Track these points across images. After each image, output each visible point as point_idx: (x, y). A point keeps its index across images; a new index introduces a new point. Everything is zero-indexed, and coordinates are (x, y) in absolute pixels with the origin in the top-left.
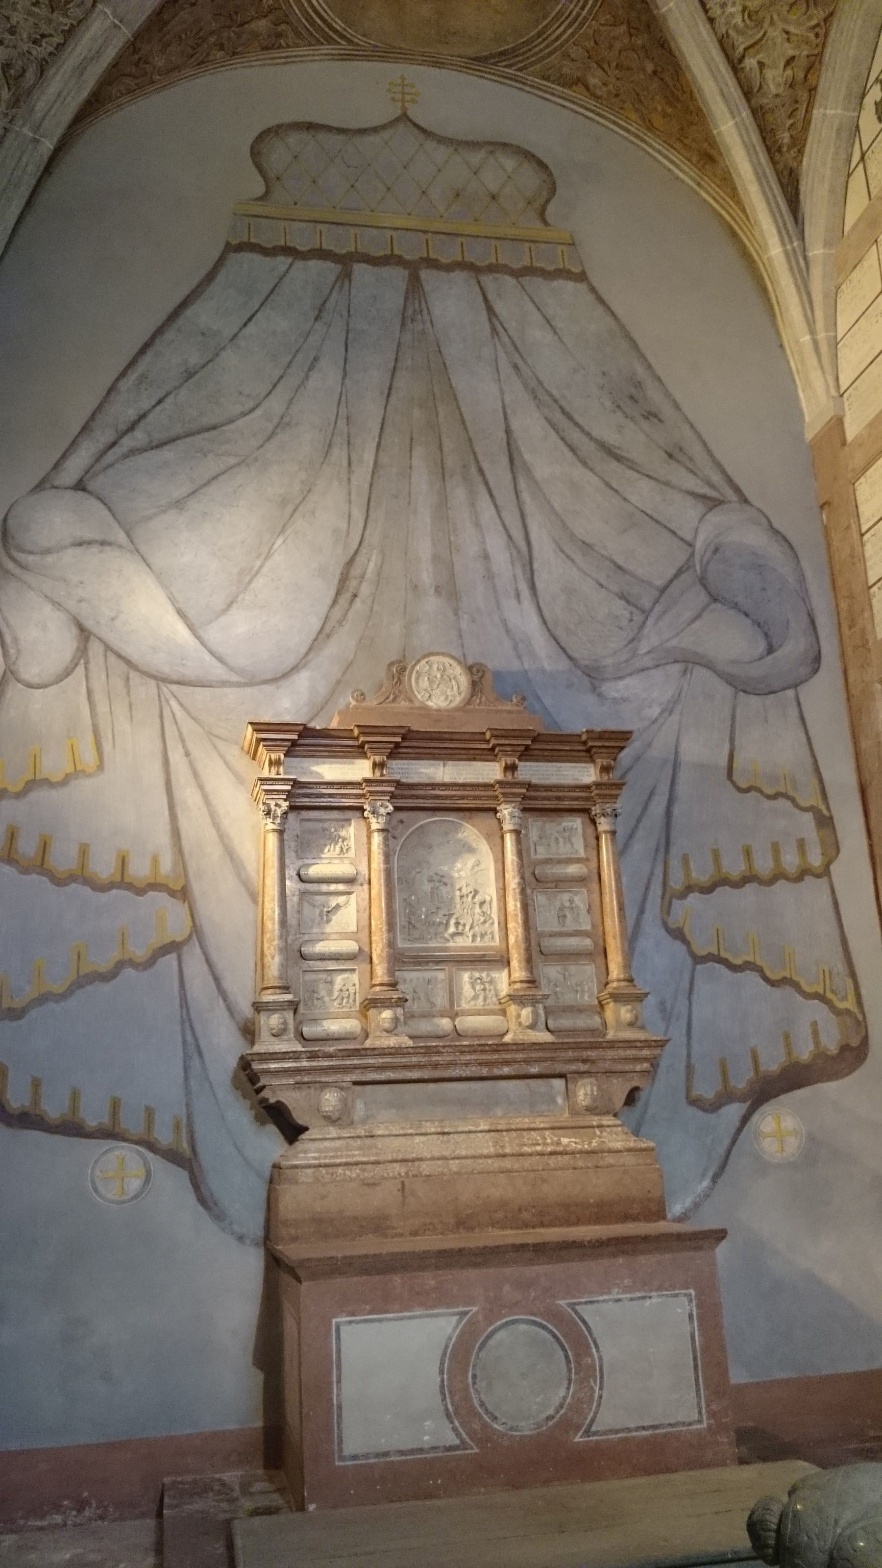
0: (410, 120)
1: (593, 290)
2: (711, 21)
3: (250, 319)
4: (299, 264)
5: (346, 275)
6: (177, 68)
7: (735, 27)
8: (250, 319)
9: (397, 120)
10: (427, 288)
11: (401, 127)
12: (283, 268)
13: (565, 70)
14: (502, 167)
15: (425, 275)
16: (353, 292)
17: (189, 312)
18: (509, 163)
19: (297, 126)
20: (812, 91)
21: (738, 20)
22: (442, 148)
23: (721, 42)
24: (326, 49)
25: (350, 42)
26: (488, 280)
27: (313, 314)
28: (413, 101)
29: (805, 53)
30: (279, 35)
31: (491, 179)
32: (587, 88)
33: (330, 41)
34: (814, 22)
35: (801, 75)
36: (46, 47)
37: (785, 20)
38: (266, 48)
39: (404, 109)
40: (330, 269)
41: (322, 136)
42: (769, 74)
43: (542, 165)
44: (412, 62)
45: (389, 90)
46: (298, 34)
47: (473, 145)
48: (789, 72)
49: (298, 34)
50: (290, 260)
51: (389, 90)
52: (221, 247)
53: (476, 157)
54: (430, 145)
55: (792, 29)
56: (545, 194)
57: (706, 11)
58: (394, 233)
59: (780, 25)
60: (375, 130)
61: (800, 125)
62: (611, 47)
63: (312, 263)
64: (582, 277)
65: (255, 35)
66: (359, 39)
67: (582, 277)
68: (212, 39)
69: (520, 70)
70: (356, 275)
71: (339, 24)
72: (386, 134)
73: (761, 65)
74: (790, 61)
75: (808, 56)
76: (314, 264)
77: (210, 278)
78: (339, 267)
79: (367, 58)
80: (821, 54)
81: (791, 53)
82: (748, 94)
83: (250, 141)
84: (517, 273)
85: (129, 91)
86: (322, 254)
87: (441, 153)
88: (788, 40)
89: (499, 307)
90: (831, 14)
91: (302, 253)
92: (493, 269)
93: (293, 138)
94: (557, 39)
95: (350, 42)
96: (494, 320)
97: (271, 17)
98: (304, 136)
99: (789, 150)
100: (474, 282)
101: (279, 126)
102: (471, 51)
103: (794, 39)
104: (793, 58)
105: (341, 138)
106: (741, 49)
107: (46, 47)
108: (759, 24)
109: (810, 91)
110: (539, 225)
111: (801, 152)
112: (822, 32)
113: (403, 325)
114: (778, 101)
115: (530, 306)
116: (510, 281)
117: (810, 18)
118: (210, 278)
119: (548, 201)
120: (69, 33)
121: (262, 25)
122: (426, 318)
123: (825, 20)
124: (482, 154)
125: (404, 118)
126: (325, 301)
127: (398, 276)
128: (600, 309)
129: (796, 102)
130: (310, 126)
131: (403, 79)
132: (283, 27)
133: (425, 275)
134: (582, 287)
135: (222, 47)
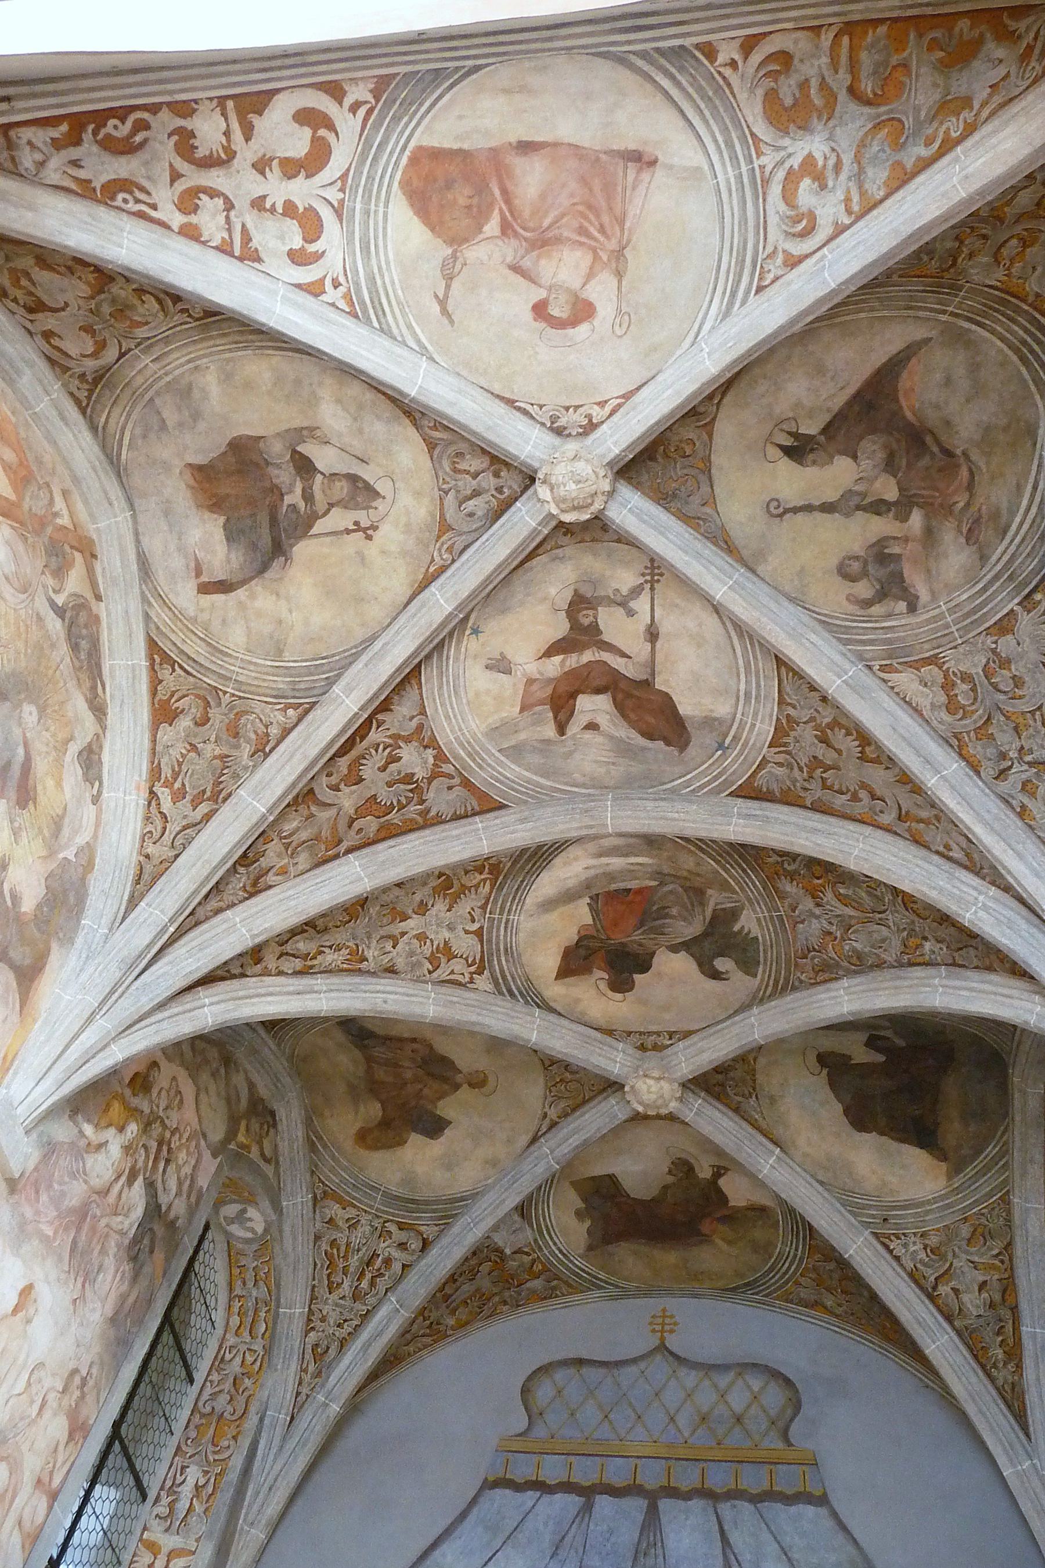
0: (667, 1349)
1: (834, 1515)
2: (897, 1258)
3: (490, 1559)
4: (546, 1498)
5: (588, 1508)
6: (467, 1323)
7: (921, 1261)
8: (490, 1559)
9: (656, 1349)
10: (664, 1519)
11: (658, 1357)
12: (530, 1504)
13: (802, 1295)
14: (749, 1387)
15: (665, 1505)
16: (592, 1526)
17: (437, 1553)
18: (756, 1383)
19: (565, 1363)
20: (1015, 1309)
21: (922, 1255)
22: (694, 1373)
23: (911, 1275)
24: (597, 1293)
25: (617, 1287)
26: (725, 1508)
27: (549, 1553)
28: (672, 1331)
29: (996, 1277)
30: (554, 1288)
31: (737, 1400)
32: (825, 1308)
33: (600, 1288)
34: (995, 1252)
35: (997, 1297)
36: (347, 1328)
37: (967, 1252)
38: (545, 1298)
39: (662, 1340)
40: (574, 1501)
41: (585, 1370)
42: (965, 1298)
43: (788, 1382)
44: (673, 1295)
45: (651, 1324)
46: (570, 1286)
47: (722, 1368)
48: (985, 1295)
49: (570, 1286)
50: (538, 1494)
51: (651, 1324)
52: (479, 1484)
53: (724, 1380)
54: (683, 1372)
55: (976, 1259)
56: (789, 1412)
57: (891, 1252)
58: (638, 1461)
59: (964, 1256)
60: (634, 1361)
61: (1011, 1341)
62: (831, 1278)
63: (558, 1496)
64: (822, 1500)
65: (533, 1292)
66: (622, 1283)
67: (822, 1500)
68: (497, 1299)
69: (766, 1296)
70: (596, 1508)
71: (602, 1275)
72: (643, 1365)
73: (956, 1291)
74: (983, 1286)
75: (999, 1280)
76: (560, 1499)
77: (463, 1515)
78: (583, 1499)
79: (634, 1296)
80: (1012, 1277)
81: (981, 1279)
82: (949, 1318)
83: (523, 1379)
84: (756, 1499)
85: (425, 1347)
86: (568, 1487)
87: (690, 1378)
88: (975, 1268)
89: (734, 1537)
90: (1009, 1244)
91: (549, 1486)
92: (735, 1495)
93: (560, 1375)
94: (785, 1274)
95: (617, 1287)
96: (728, 1551)
97: (542, 1277)
98: (572, 1371)
99: (1005, 1364)
100: (711, 1510)
101: (550, 1364)
102: (720, 1284)
103: (980, 1266)
104: (985, 1283)
105: (602, 1371)
106: (932, 1279)
107: (347, 1328)
108: (943, 1257)
109: (1012, 1309)
110: (781, 1445)
111: (1019, 1366)
112: (1006, 1258)
113: (635, 1559)
114: (981, 1321)
115: (766, 1536)
116: (746, 1507)
117: (990, 1249)
118: (463, 1515)
119: (792, 1420)
120: (366, 1316)
121: (537, 1284)
122: (660, 1551)
123: (1006, 1248)
124: (732, 1374)
125: (662, 1348)
126: (563, 1538)
127: (636, 1506)
128: (840, 1538)
129: (1001, 1320)
130: (580, 1362)
131: (664, 1310)
132: (555, 1282)
133: (665, 1505)
134: (823, 1511)
135: (505, 1303)
